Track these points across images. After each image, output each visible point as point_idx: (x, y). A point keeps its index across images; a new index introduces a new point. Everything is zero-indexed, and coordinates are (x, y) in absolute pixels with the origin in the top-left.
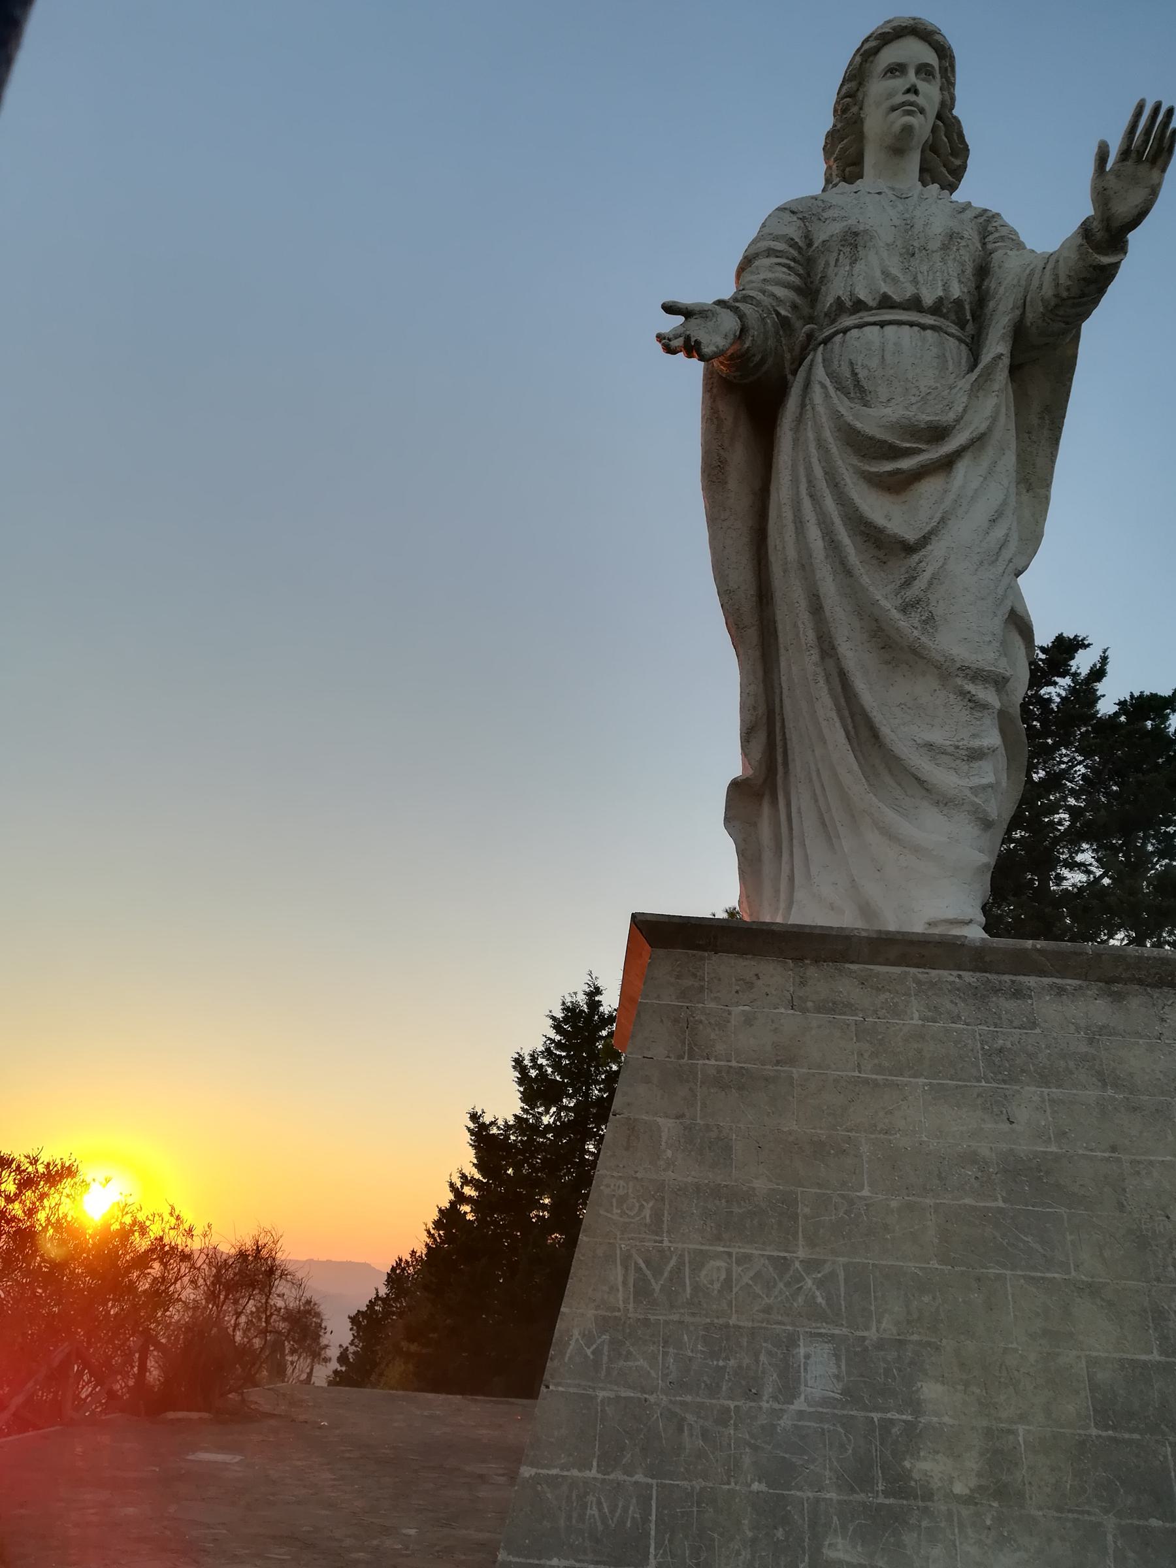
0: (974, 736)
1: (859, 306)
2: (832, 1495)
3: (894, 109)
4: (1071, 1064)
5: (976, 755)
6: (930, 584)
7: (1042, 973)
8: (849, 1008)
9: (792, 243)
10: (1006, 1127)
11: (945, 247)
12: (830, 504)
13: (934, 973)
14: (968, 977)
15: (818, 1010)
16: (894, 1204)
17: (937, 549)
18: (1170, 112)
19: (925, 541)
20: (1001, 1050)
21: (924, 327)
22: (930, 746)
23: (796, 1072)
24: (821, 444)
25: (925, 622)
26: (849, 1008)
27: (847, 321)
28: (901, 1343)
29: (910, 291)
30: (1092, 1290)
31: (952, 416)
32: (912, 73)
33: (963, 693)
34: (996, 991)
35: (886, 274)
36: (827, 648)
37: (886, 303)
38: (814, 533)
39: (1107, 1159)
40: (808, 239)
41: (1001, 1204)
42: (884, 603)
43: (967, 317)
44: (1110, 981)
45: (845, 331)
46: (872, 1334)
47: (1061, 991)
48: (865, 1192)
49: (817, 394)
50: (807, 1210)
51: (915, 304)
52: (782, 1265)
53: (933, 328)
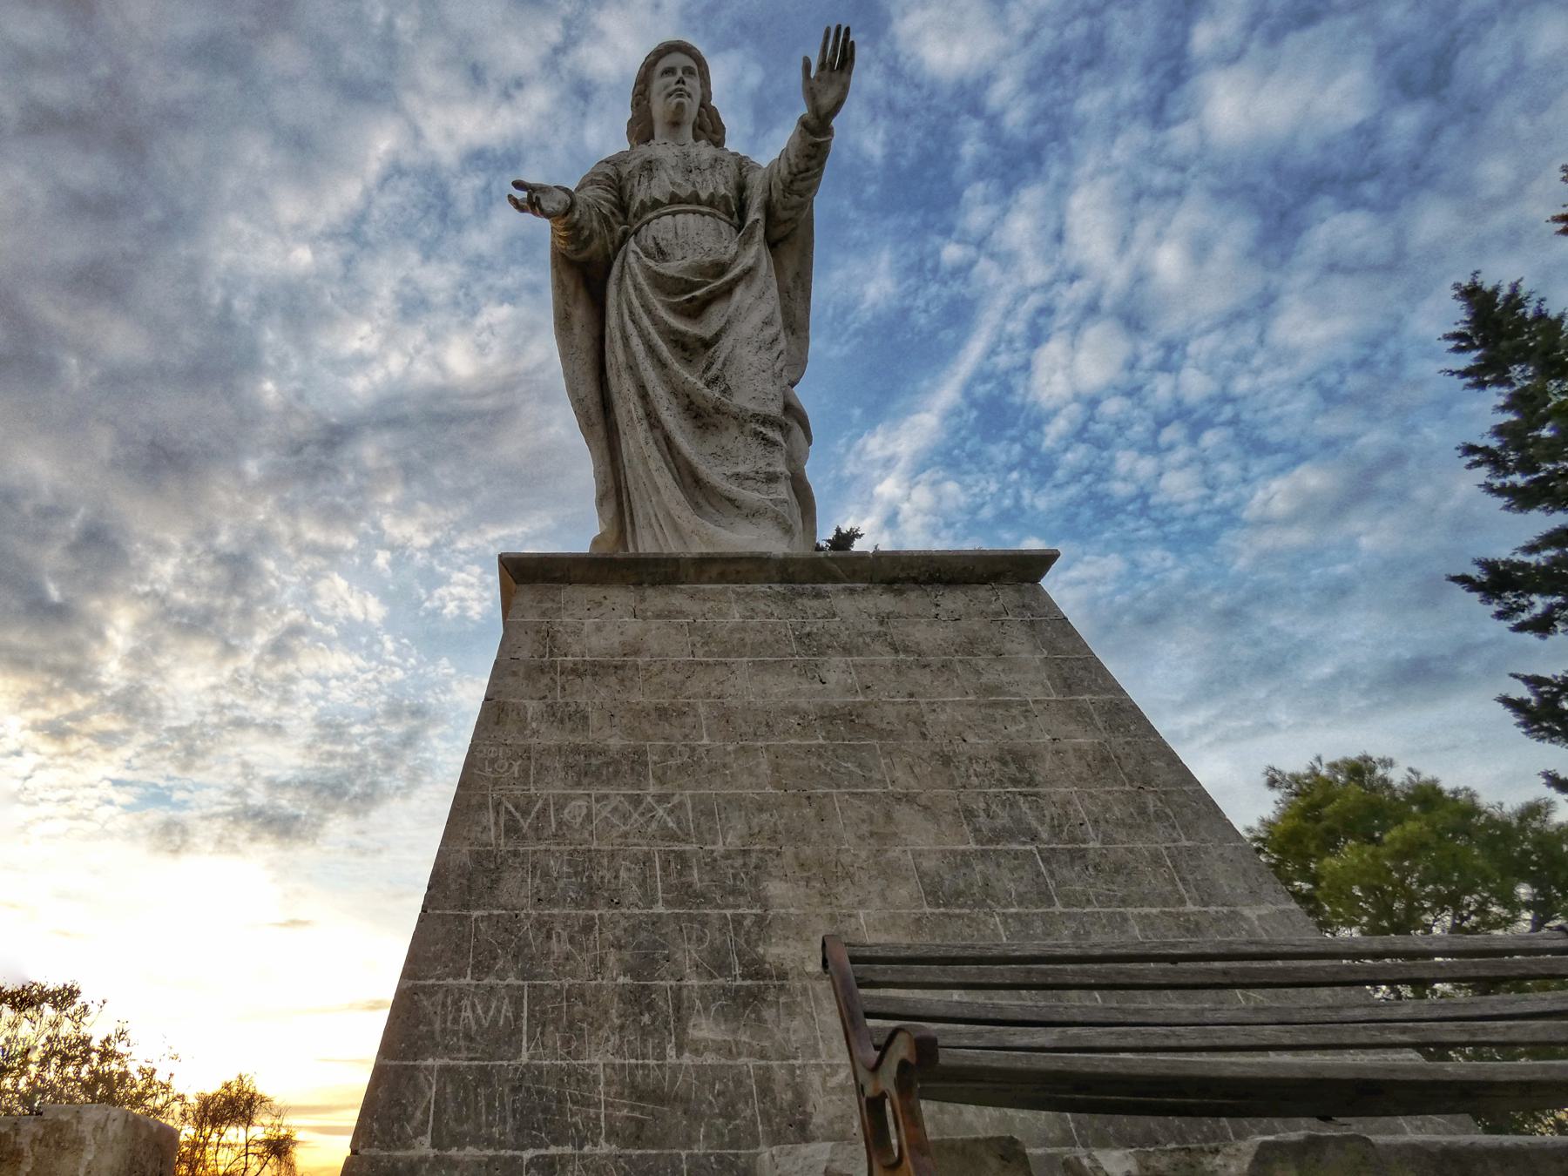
1: (656, 204)
2: (694, 982)
3: (670, 95)
4: (868, 640)
5: (772, 478)
6: (724, 364)
7: (836, 580)
9: (607, 176)
10: (819, 686)
11: (712, 166)
12: (646, 322)
13: (749, 587)
14: (777, 587)
15: (658, 616)
16: (730, 748)
17: (726, 344)
18: (848, 30)
19: (717, 337)
20: (809, 634)
21: (703, 214)
25: (724, 391)
26: (681, 613)
27: (650, 216)
28: (745, 853)
29: (690, 189)
31: (727, 257)
32: (680, 73)
34: (801, 595)
35: (673, 184)
36: (653, 420)
37: (674, 199)
38: (636, 343)
40: (619, 175)
41: (821, 741)
42: (692, 379)
43: (734, 209)
45: (648, 223)
46: (719, 848)
47: (852, 591)
48: (705, 741)
49: (632, 258)
50: (655, 758)
52: (636, 801)
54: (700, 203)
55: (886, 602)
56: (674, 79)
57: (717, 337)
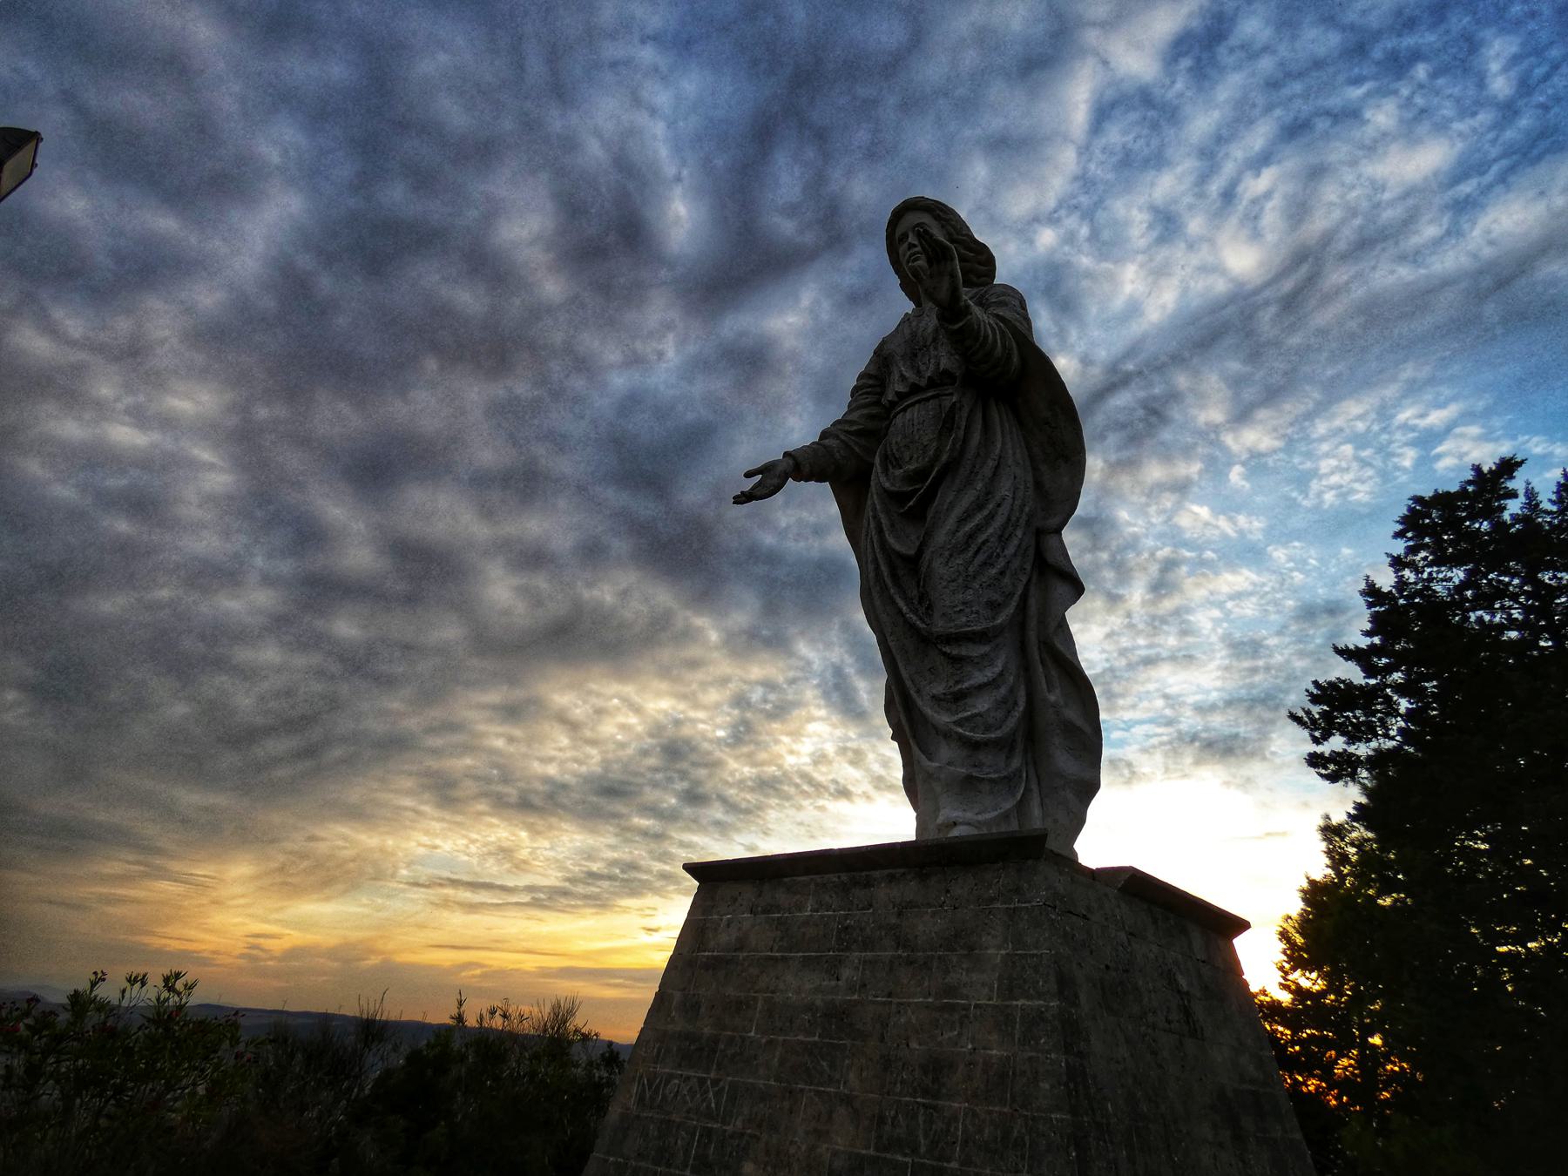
0: (957, 682)
8: (778, 908)
10: (833, 983)
11: (935, 340)
14: (844, 877)
17: (927, 556)
19: (920, 552)
21: (927, 400)
23: (742, 955)
24: (874, 509)
28: (742, 1134)
30: (848, 1100)
33: (945, 654)
37: (901, 396)
39: (884, 1003)
46: (729, 1128)
47: (891, 879)
51: (915, 389)
55: (910, 889)
56: (905, 245)
57: (920, 552)
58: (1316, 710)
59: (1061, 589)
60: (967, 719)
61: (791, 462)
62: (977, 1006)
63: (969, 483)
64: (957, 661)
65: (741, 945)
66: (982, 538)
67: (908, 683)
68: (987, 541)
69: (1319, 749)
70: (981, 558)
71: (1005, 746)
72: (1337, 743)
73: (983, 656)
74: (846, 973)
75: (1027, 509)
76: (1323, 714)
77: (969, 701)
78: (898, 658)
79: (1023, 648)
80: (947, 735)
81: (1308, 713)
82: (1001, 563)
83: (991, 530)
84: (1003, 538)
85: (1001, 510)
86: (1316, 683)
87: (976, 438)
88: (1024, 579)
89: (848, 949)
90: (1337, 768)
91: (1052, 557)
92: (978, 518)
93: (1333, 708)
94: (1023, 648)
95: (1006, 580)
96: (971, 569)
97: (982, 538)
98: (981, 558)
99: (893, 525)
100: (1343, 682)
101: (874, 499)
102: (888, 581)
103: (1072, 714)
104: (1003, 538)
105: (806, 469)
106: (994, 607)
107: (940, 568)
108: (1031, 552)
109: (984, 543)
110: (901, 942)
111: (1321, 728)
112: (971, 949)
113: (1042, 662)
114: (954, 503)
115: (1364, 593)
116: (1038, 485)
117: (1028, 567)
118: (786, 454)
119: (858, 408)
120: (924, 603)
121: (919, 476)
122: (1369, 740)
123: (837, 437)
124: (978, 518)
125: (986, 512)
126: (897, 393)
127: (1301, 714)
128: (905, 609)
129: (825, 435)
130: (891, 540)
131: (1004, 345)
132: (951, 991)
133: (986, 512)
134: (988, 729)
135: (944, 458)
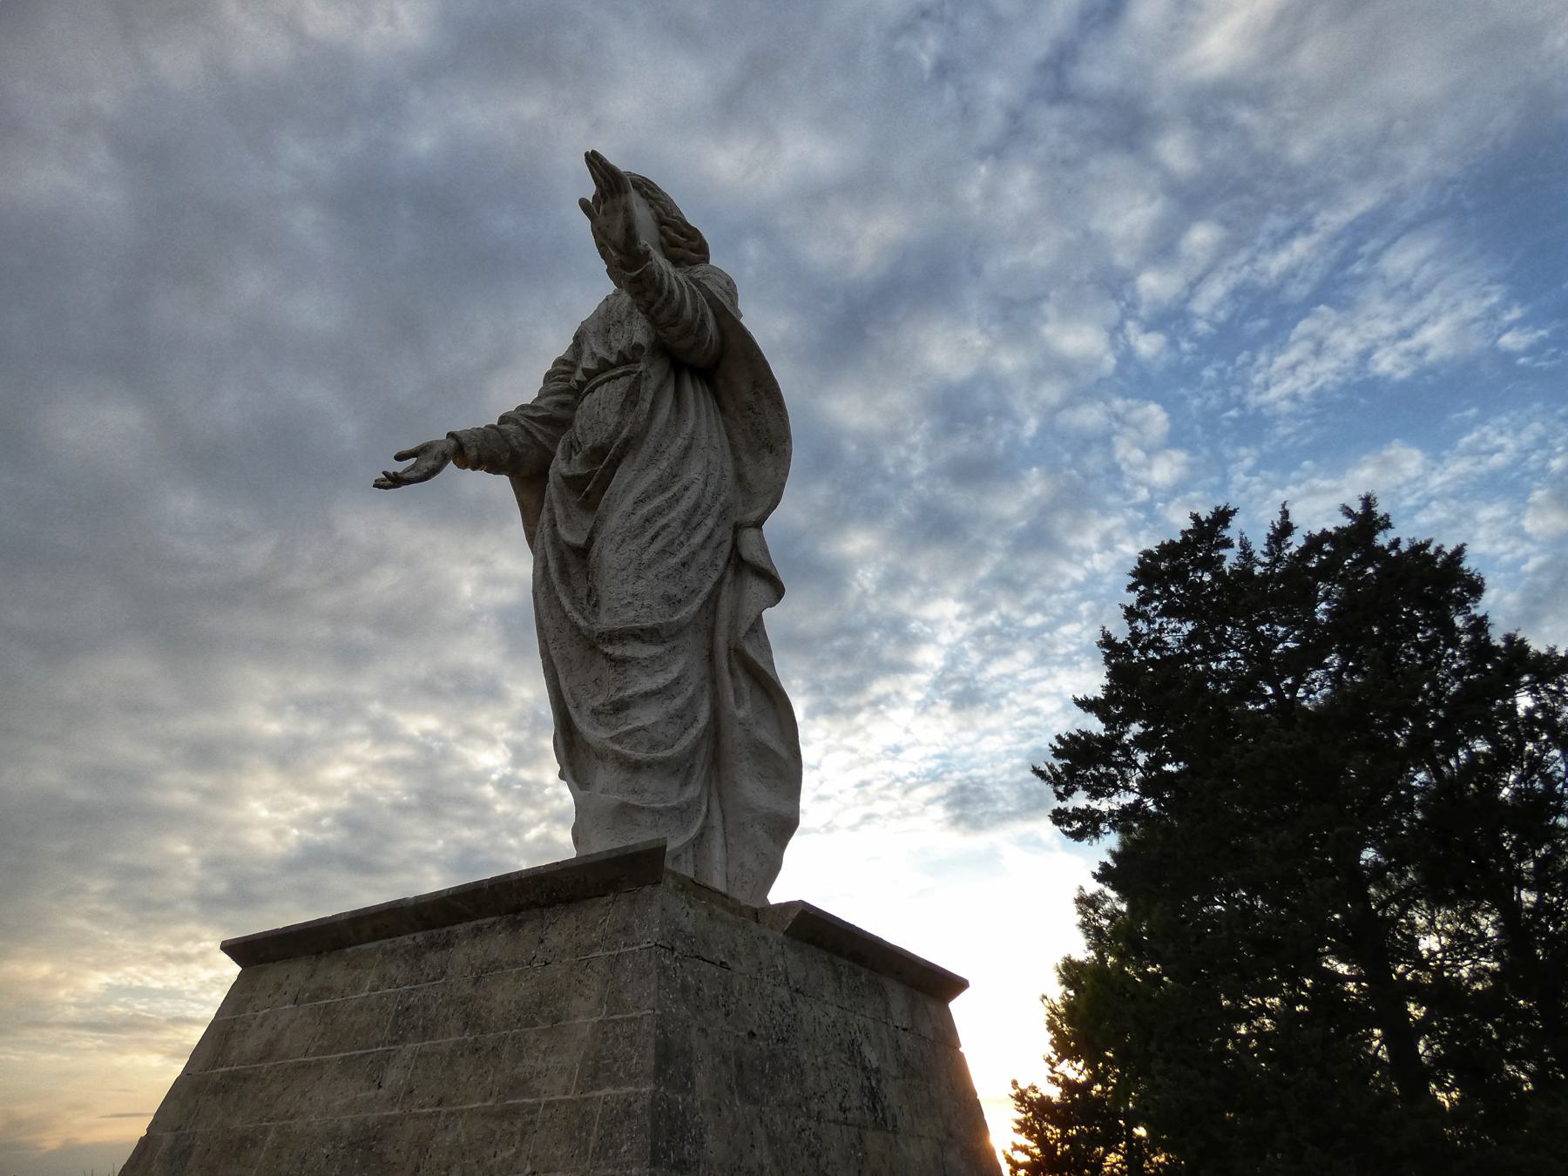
0: (619, 689)
7: (470, 918)
11: (629, 314)
14: (420, 937)
17: (597, 545)
19: (591, 540)
22: (594, 712)
39: (430, 1116)
44: (517, 910)
51: (605, 366)
53: (623, 374)
54: (613, 367)
55: (498, 944)
57: (591, 540)
58: (1058, 764)
59: (756, 588)
60: (629, 734)
61: (453, 442)
62: (549, 1105)
63: (652, 461)
64: (619, 663)
65: (269, 1052)
66: (662, 521)
67: (567, 697)
68: (666, 526)
69: (1062, 805)
70: (659, 544)
71: (679, 769)
72: (1080, 800)
73: (654, 659)
74: (394, 1076)
75: (722, 499)
76: (1066, 768)
77: (632, 712)
78: (559, 668)
79: (711, 657)
80: (601, 756)
81: (1051, 767)
82: (684, 553)
83: (673, 514)
84: (689, 525)
85: (688, 494)
86: (1059, 738)
87: (664, 413)
88: (715, 576)
89: (403, 1039)
90: (1083, 826)
91: (749, 551)
92: (658, 501)
93: (1078, 762)
94: (711, 657)
95: (691, 574)
96: (645, 557)
97: (662, 521)
98: (659, 544)
99: (568, 516)
100: (1083, 734)
101: (551, 490)
102: (555, 577)
103: (767, 734)
104: (689, 525)
105: (473, 453)
106: (673, 602)
107: (609, 556)
108: (727, 547)
109: (664, 528)
110: (471, 1021)
111: (1064, 781)
112: (556, 1020)
113: (732, 673)
114: (630, 485)
115: (1100, 644)
116: (740, 478)
117: (721, 563)
118: (451, 435)
119: (547, 395)
120: (592, 601)
121: (598, 452)
122: (1110, 795)
123: (516, 422)
124: (658, 501)
125: (668, 494)
126: (585, 371)
127: (1044, 768)
128: (568, 607)
129: (504, 419)
130: (562, 531)
131: (694, 305)
132: (519, 1085)
133: (668, 494)
134: (654, 746)
135: (624, 433)
